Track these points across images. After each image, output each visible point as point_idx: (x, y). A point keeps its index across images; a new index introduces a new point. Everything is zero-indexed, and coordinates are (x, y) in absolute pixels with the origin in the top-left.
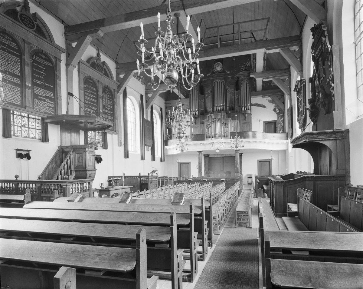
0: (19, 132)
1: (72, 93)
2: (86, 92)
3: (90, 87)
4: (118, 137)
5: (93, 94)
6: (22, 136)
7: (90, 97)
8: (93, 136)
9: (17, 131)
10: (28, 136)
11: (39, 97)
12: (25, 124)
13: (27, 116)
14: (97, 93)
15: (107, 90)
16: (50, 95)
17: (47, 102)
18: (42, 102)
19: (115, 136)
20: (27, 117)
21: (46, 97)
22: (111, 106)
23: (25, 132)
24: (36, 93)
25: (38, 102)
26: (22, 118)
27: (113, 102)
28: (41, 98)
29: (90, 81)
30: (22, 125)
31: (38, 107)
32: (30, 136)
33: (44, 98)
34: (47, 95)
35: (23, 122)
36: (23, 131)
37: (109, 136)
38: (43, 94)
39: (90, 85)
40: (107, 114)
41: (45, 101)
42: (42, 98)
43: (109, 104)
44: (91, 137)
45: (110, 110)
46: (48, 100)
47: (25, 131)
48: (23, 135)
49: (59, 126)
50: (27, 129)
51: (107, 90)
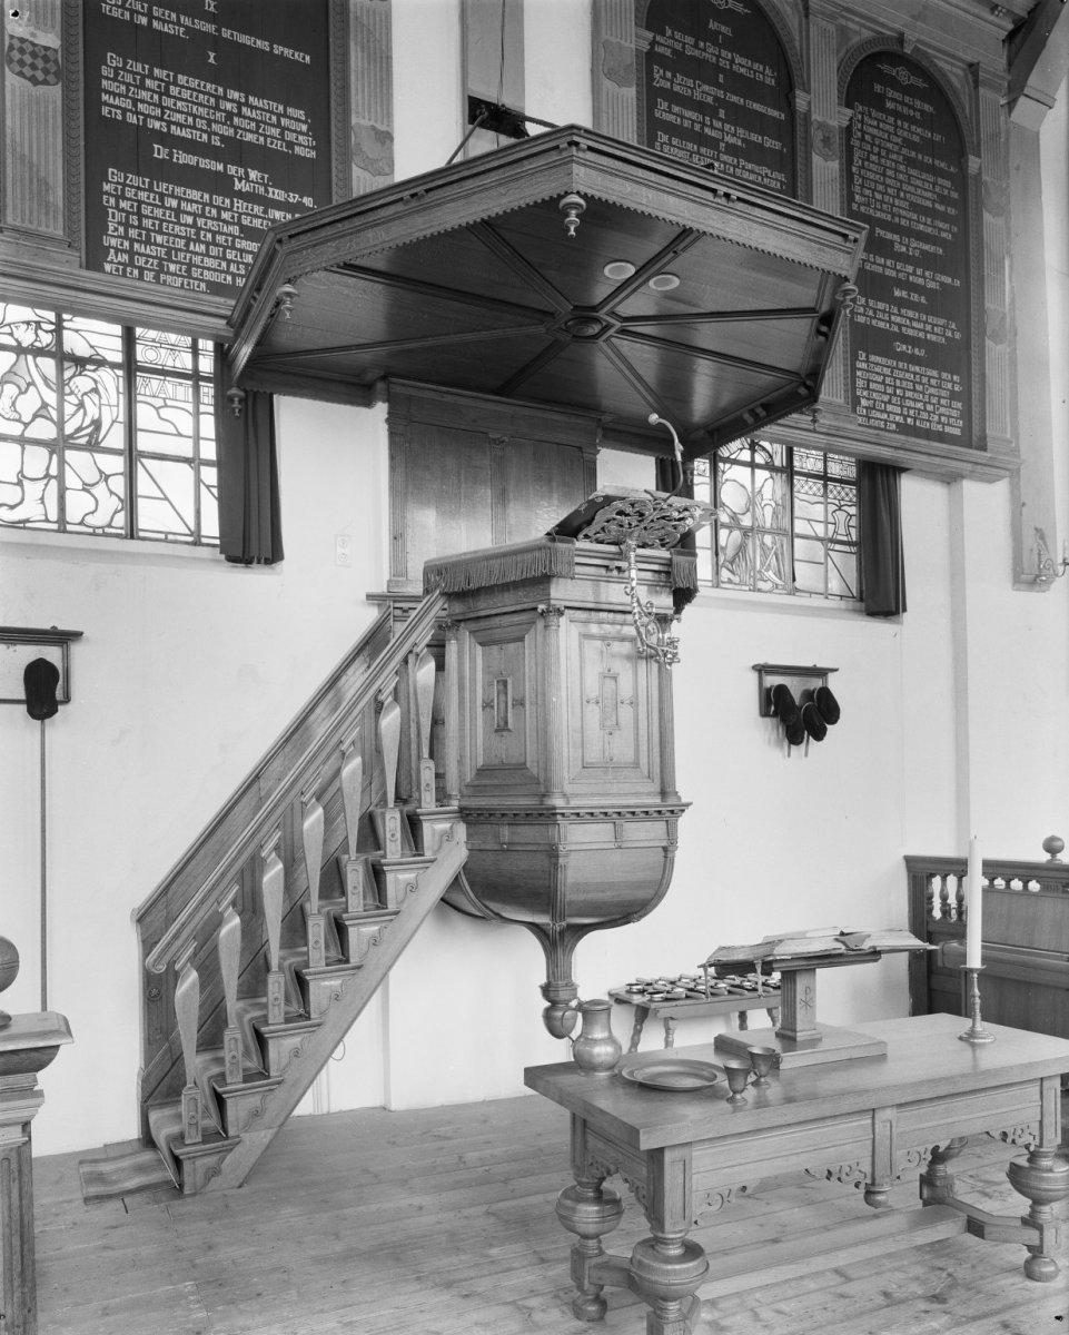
0: (33, 490)
1: (508, 101)
2: (673, 98)
3: (709, 52)
4: (1017, 505)
5: (739, 116)
6: (62, 520)
7: (712, 143)
8: (768, 512)
9: (20, 483)
10: (120, 519)
11: (160, 152)
12: (97, 424)
13: (118, 358)
14: (788, 104)
15: (892, 83)
16: (275, 132)
17: (241, 195)
18: (194, 194)
19: (986, 501)
20: (114, 366)
21: (237, 151)
22: (944, 217)
23: (101, 490)
24: (132, 119)
25: (143, 195)
26: (67, 374)
27: (962, 181)
28: (183, 158)
30: (69, 429)
31: (148, 242)
32: (143, 522)
33: (205, 164)
34: (250, 137)
35: (81, 405)
36: (71, 480)
37: (917, 499)
38: (201, 123)
39: (712, 37)
40: (897, 293)
41: (221, 184)
42: (191, 160)
43: (914, 207)
44: (746, 521)
45: (926, 261)
46: (253, 174)
47: (92, 477)
48: (73, 514)
49: (374, 420)
50: (116, 464)
51: (892, 83)
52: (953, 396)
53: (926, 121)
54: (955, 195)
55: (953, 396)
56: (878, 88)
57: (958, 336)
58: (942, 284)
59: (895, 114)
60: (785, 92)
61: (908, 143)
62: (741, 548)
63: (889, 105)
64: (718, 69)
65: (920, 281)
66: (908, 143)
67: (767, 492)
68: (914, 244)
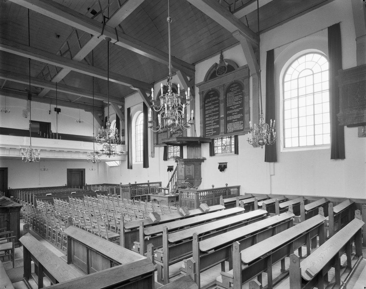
5: (213, 104)
15: (233, 87)
29: (212, 93)
40: (233, 114)
43: (236, 102)
44: (225, 145)
45: (238, 108)
52: (242, 124)
53: (238, 89)
54: (242, 96)
55: (242, 124)
56: (230, 89)
57: (242, 115)
58: (240, 110)
59: (233, 91)
60: (218, 99)
61: (235, 94)
62: (225, 148)
63: (232, 90)
64: (211, 101)
65: (236, 111)
66: (235, 94)
67: (228, 141)
68: (235, 106)
